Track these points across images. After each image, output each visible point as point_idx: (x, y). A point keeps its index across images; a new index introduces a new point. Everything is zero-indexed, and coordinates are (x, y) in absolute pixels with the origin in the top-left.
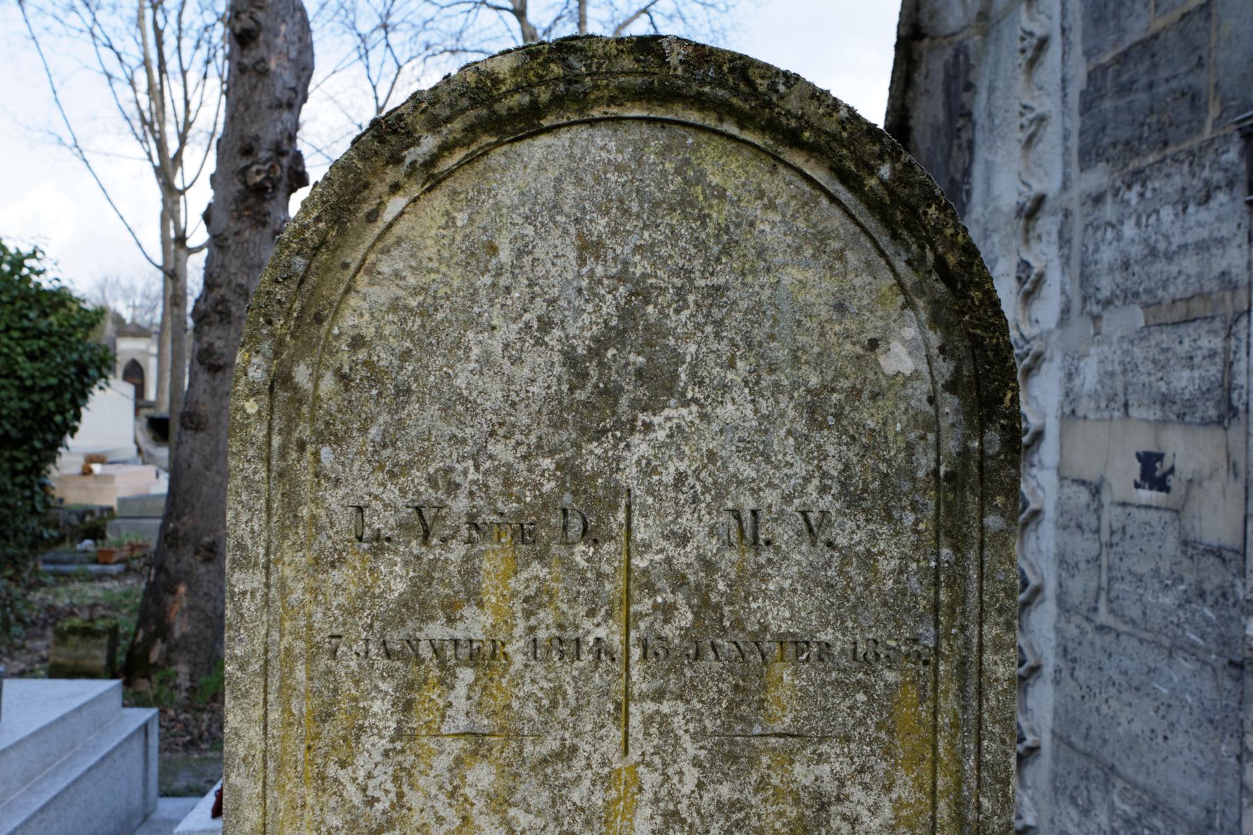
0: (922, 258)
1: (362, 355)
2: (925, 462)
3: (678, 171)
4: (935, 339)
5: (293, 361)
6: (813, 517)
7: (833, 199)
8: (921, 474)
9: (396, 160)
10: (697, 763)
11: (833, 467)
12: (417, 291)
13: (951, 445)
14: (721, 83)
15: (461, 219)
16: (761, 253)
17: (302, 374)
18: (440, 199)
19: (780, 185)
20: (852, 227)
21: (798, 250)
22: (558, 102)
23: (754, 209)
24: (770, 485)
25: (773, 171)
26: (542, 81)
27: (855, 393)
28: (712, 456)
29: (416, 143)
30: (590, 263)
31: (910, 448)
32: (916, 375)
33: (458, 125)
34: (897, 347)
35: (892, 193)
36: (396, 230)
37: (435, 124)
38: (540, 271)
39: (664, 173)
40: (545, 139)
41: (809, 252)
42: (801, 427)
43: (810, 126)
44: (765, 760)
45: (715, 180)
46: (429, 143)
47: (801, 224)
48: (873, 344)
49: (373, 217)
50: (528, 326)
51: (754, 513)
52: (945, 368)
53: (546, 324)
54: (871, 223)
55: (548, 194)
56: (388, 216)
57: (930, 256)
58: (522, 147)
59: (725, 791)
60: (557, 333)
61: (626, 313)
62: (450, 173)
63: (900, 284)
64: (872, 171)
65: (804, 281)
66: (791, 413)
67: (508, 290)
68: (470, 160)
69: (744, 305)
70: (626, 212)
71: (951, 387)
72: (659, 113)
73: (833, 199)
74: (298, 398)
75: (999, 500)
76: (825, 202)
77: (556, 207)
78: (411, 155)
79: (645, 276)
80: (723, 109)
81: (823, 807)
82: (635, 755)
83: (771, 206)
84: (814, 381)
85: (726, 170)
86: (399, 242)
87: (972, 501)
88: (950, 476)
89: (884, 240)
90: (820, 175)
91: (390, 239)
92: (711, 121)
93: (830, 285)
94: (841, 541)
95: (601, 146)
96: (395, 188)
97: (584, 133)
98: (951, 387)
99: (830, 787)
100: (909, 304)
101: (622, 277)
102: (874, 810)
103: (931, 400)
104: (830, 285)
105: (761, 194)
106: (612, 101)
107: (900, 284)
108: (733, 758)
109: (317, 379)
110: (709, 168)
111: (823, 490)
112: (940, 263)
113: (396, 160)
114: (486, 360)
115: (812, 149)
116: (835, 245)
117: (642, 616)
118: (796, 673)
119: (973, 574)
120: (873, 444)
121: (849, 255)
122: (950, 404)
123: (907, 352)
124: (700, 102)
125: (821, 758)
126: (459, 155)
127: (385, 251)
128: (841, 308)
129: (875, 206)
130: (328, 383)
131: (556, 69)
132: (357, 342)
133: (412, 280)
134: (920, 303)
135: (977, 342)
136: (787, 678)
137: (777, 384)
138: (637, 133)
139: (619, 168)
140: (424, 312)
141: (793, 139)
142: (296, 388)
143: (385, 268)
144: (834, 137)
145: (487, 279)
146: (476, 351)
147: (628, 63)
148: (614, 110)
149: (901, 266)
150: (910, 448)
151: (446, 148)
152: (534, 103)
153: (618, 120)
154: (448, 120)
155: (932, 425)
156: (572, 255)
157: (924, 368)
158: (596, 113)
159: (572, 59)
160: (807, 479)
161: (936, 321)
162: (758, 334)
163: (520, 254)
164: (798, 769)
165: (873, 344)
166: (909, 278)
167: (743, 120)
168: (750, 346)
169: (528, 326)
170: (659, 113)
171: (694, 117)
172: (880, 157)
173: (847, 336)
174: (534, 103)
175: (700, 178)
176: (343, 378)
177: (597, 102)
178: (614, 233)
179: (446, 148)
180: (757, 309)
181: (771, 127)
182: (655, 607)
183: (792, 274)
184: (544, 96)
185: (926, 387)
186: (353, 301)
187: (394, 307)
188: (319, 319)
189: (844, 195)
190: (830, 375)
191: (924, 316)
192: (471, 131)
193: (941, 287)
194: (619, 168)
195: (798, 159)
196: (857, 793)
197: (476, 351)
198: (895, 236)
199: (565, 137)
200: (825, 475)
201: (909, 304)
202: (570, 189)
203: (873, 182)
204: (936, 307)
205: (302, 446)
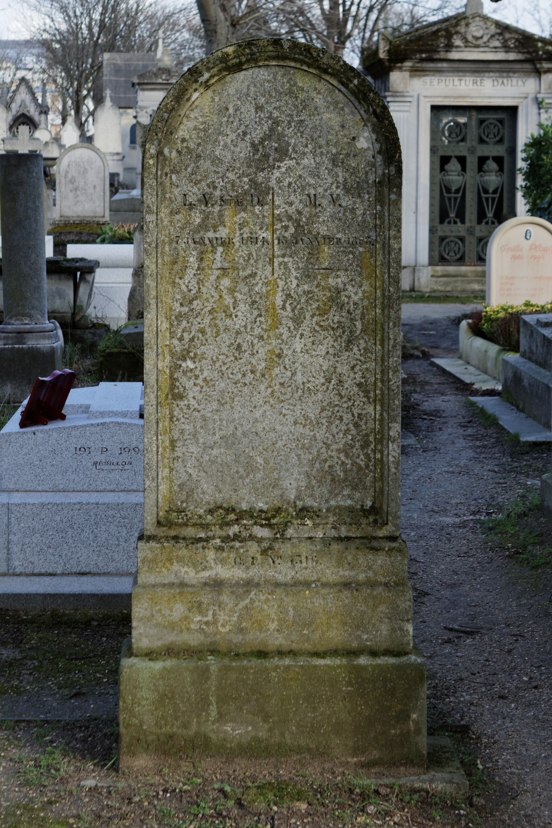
0: (369, 110)
1: (185, 144)
2: (372, 178)
3: (288, 82)
4: (374, 136)
5: (164, 147)
6: (334, 196)
7: (340, 90)
8: (370, 182)
9: (196, 81)
10: (296, 278)
11: (341, 179)
12: (202, 123)
13: (380, 172)
14: (301, 54)
15: (217, 99)
16: (316, 109)
17: (166, 151)
18: (210, 93)
19: (322, 86)
20: (346, 100)
21: (328, 107)
22: (248, 61)
23: (314, 94)
24: (320, 186)
25: (320, 81)
26: (243, 54)
27: (348, 155)
28: (300, 176)
29: (202, 76)
30: (259, 113)
31: (367, 173)
32: (368, 149)
33: (216, 69)
34: (362, 139)
35: (358, 89)
36: (196, 103)
37: (208, 69)
38: (243, 116)
39: (283, 83)
40: (244, 72)
41: (332, 108)
42: (330, 166)
43: (331, 67)
44: (319, 277)
45: (300, 84)
46: (206, 75)
47: (329, 99)
48: (354, 138)
49: (188, 100)
50: (239, 134)
51: (315, 195)
52: (377, 146)
53: (245, 134)
54: (352, 98)
55: (245, 90)
56: (193, 99)
57: (371, 109)
58: (236, 75)
59: (306, 287)
60: (249, 136)
61: (271, 130)
62: (213, 84)
63: (362, 118)
64: (351, 82)
65: (331, 118)
66: (326, 162)
67: (232, 122)
68: (219, 80)
69: (310, 126)
70: (271, 96)
71: (379, 152)
72: (281, 63)
73: (340, 90)
74: (165, 159)
75: (395, 190)
76: (337, 91)
77: (248, 95)
78: (202, 79)
79: (277, 117)
80: (302, 62)
81: (339, 293)
82: (276, 276)
83: (319, 93)
84: (334, 151)
85: (304, 81)
86: (196, 107)
87: (386, 190)
88: (380, 182)
89: (357, 104)
90: (335, 83)
91: (194, 106)
92: (298, 66)
93: (339, 119)
94: (344, 204)
95: (262, 74)
96: (196, 90)
97: (257, 70)
98: (379, 152)
99: (341, 286)
100: (365, 125)
101: (270, 118)
102: (356, 293)
103: (373, 157)
104: (339, 119)
105: (316, 89)
106: (266, 60)
107: (362, 118)
108: (308, 276)
109: (171, 152)
110: (298, 80)
111: (338, 187)
112: (374, 112)
113: (196, 81)
114: (225, 146)
115: (332, 75)
116: (341, 105)
117: (277, 229)
118: (329, 248)
119: (387, 214)
120: (354, 172)
121: (346, 109)
122: (379, 158)
123: (365, 141)
124: (295, 60)
125: (338, 276)
126: (216, 78)
127: (192, 110)
128: (343, 126)
129: (353, 93)
130: (174, 154)
131: (247, 51)
132: (183, 140)
133: (201, 120)
134: (369, 125)
135: (387, 138)
136: (326, 250)
137: (322, 152)
138: (274, 70)
139: (269, 81)
140: (205, 130)
141: (325, 71)
142: (164, 156)
143: (192, 116)
144: (339, 71)
145: (225, 119)
146: (222, 143)
147: (270, 48)
148: (266, 63)
149: (362, 112)
150: (367, 173)
151: (212, 77)
152: (240, 62)
153: (268, 66)
154: (213, 68)
155: (374, 165)
156: (253, 110)
157: (371, 146)
158: (261, 64)
159: (253, 48)
160: (332, 184)
161: (374, 131)
162: (315, 136)
163: (236, 110)
164: (330, 280)
165: (354, 138)
166: (365, 116)
167: (309, 66)
168: (312, 140)
169: (239, 134)
170: (281, 63)
171: (293, 64)
172: (354, 77)
173: (345, 136)
174: (240, 62)
175: (295, 84)
176: (179, 152)
177: (261, 60)
178: (267, 103)
179: (212, 77)
180: (315, 127)
181: (318, 67)
182: (282, 226)
183: (326, 116)
184: (244, 59)
185: (372, 153)
186: (182, 127)
187: (195, 128)
188: (171, 133)
189: (343, 89)
190: (339, 149)
191: (370, 129)
192: (220, 71)
193: (375, 119)
194: (269, 81)
195: (328, 78)
196: (350, 288)
197: (222, 143)
198: (360, 103)
199: (251, 71)
200: (338, 182)
201: (365, 125)
202: (252, 89)
203: (352, 85)
204: (374, 125)
205: (166, 174)
